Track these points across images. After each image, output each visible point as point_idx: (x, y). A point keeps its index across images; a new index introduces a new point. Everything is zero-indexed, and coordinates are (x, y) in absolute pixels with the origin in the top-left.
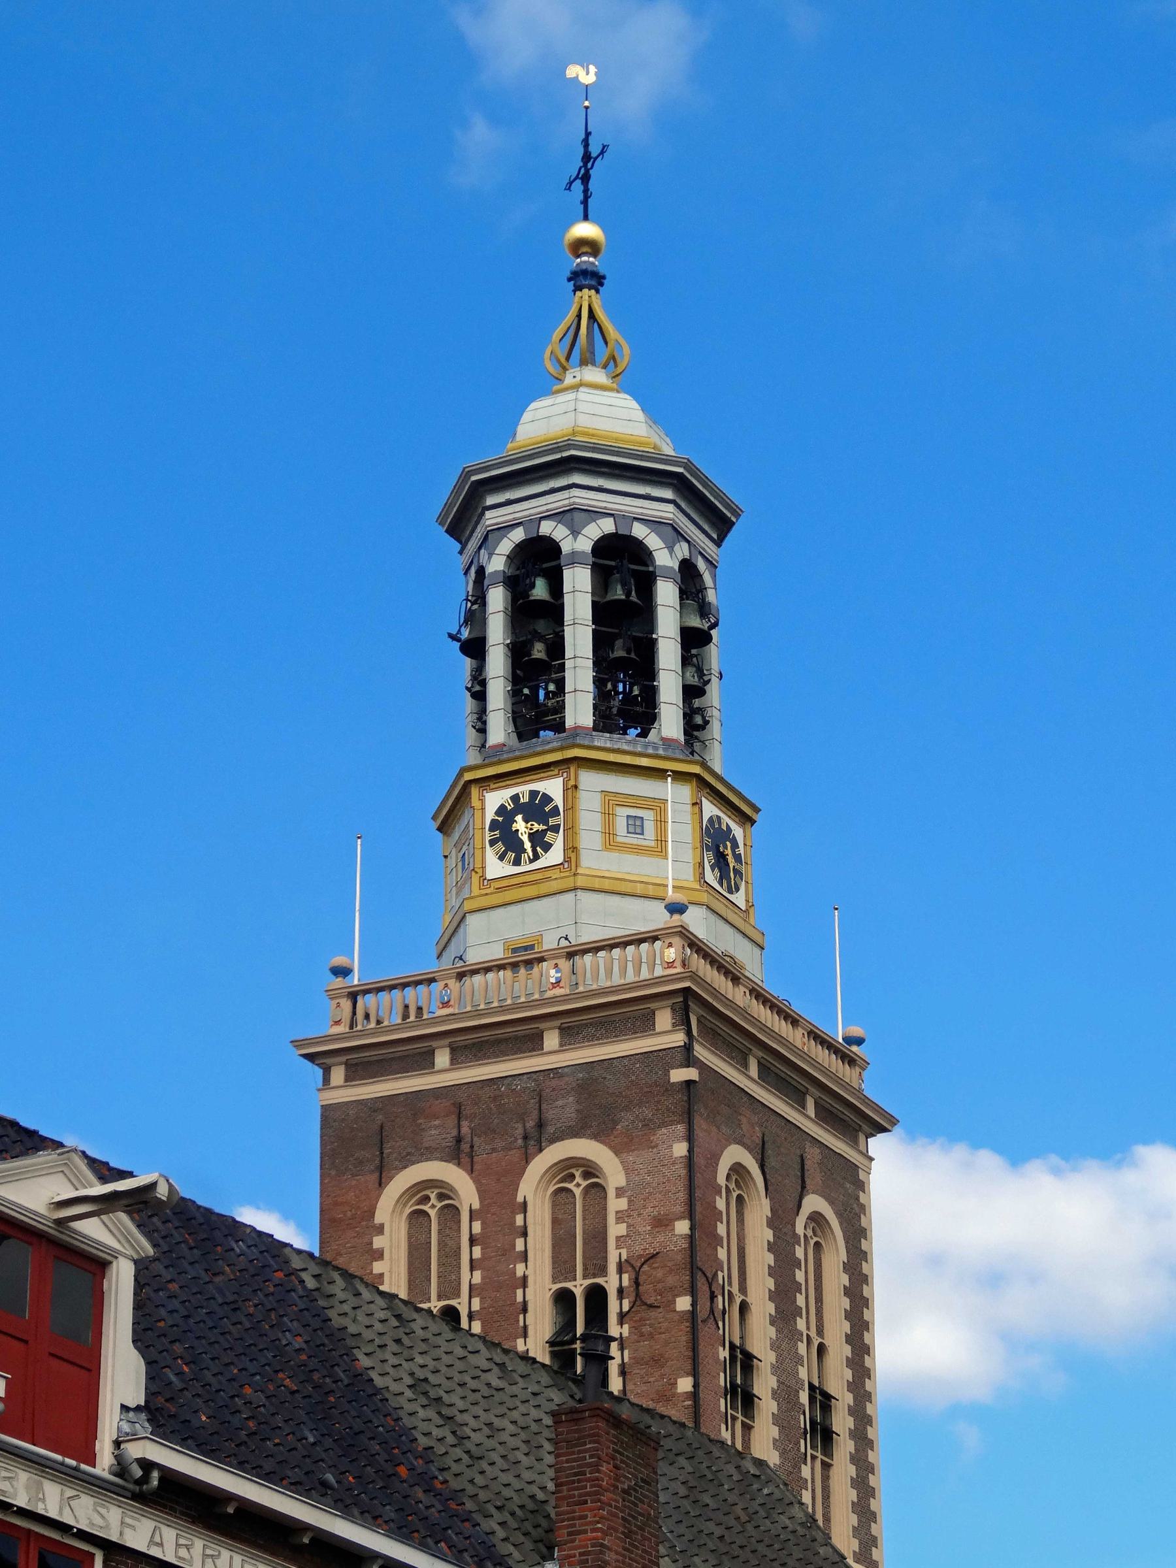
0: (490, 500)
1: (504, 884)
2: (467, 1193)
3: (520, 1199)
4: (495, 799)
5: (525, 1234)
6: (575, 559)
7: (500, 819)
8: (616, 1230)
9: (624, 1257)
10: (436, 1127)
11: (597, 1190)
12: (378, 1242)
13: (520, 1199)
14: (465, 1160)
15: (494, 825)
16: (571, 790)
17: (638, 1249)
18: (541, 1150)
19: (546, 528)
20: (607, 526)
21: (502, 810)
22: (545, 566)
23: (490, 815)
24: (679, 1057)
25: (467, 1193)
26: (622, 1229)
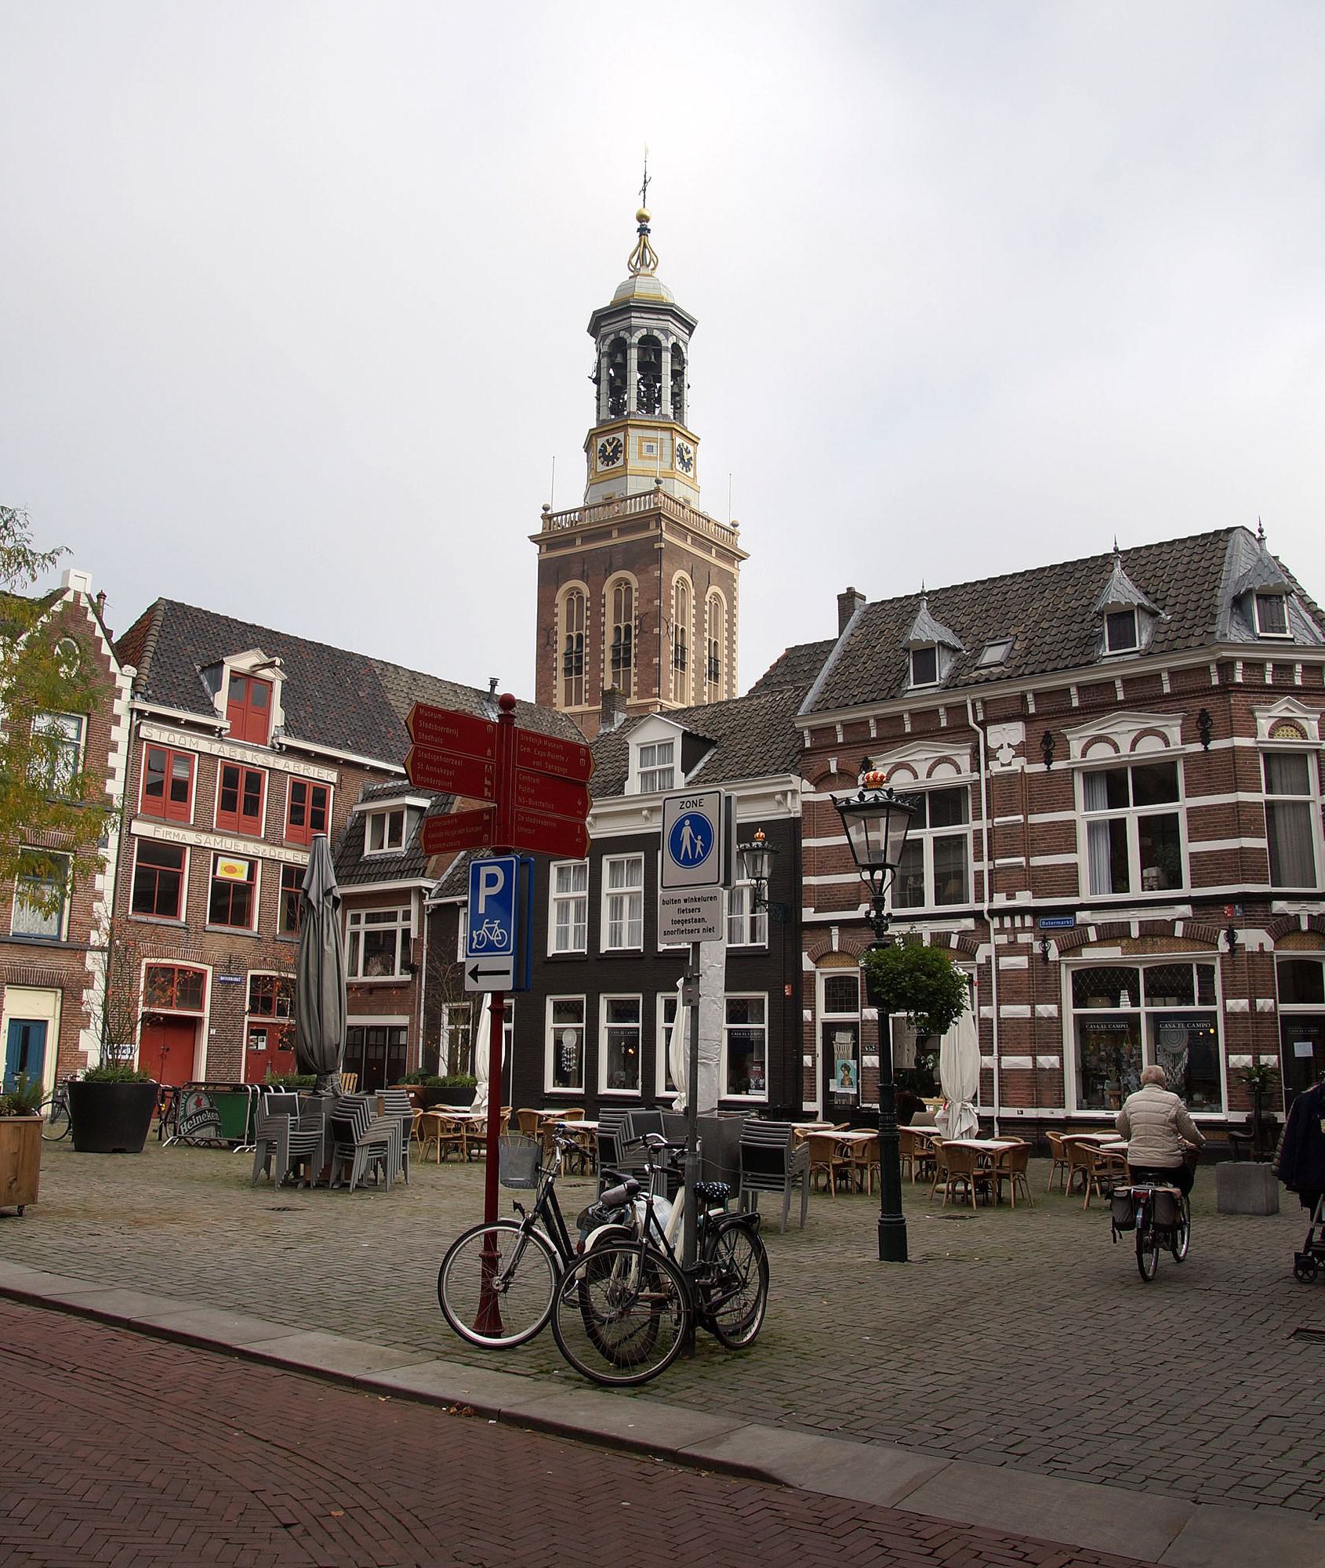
1: (604, 473)
2: (586, 593)
4: (601, 441)
8: (635, 604)
11: (629, 590)
19: (622, 334)
20: (644, 332)
25: (586, 593)
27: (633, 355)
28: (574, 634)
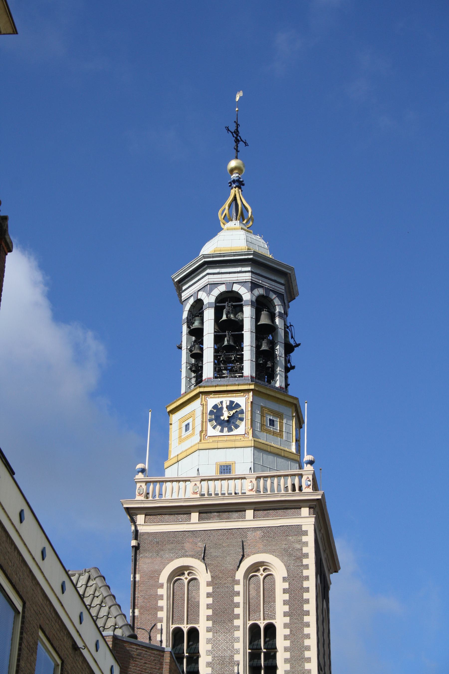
7: (215, 411)
15: (211, 413)
19: (236, 288)
21: (215, 407)
22: (234, 304)
23: (210, 408)
27: (248, 313)
28: (185, 628)
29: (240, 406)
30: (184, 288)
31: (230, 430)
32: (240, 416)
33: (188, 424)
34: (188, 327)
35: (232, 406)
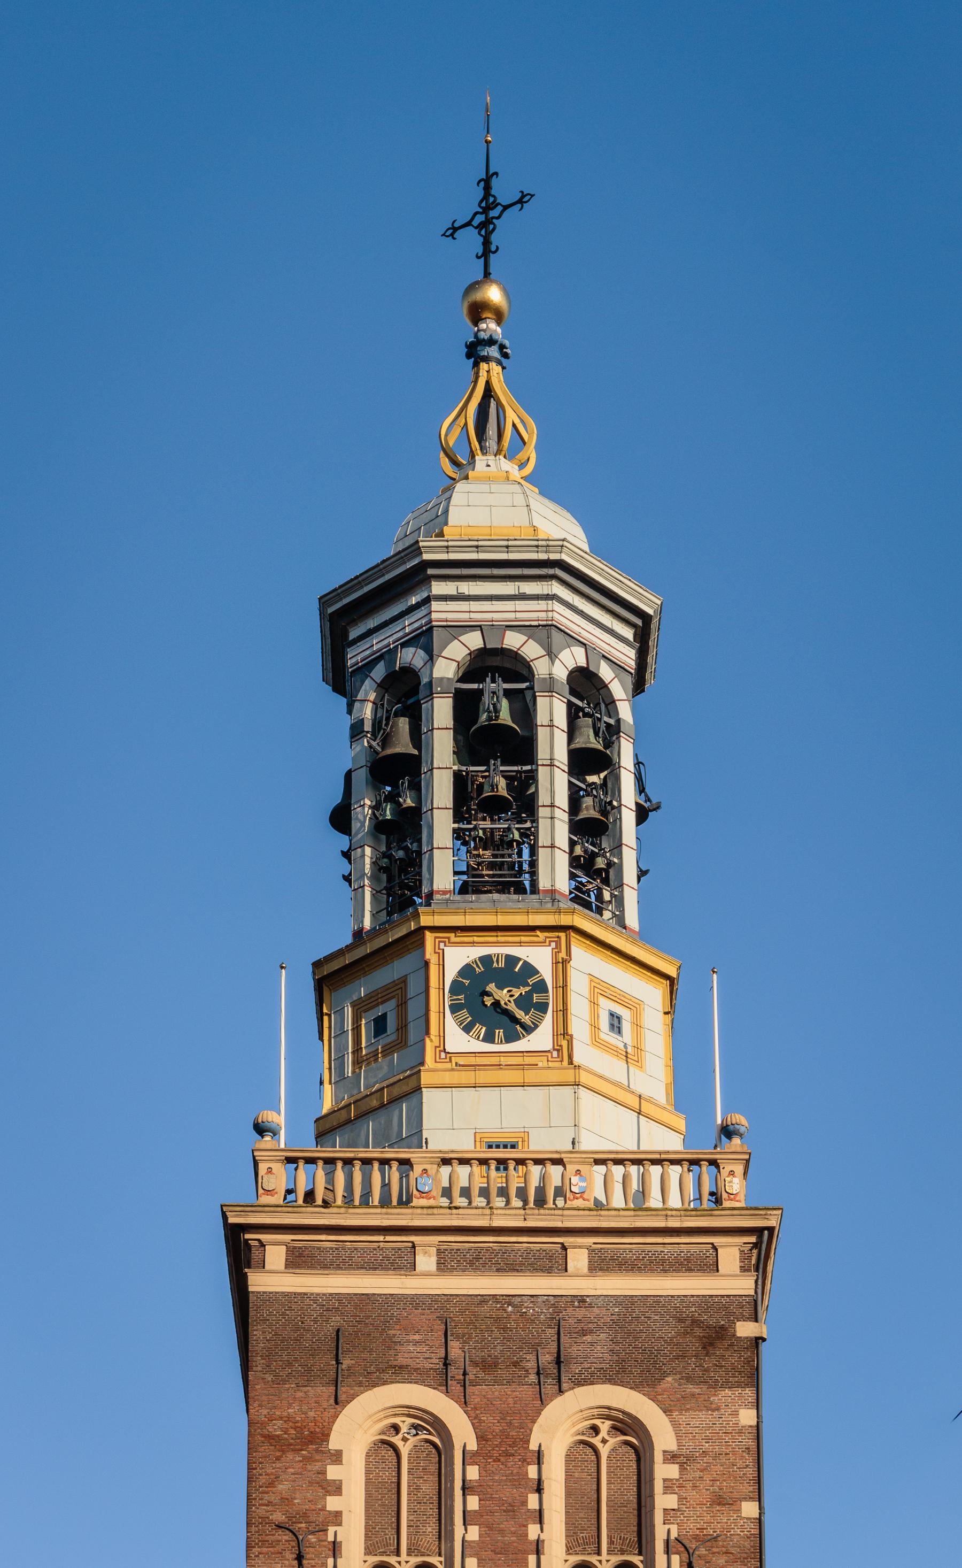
0: (438, 588)
2: (463, 1433)
3: (533, 1446)
5: (539, 1490)
6: (550, 686)
7: (467, 982)
8: (663, 1501)
9: (674, 1534)
10: (416, 1343)
11: (642, 1453)
12: (333, 1472)
13: (533, 1446)
14: (456, 1387)
16: (562, 964)
17: (692, 1527)
18: (561, 1391)
19: (513, 640)
23: (451, 974)
24: (748, 1311)
25: (463, 1433)
26: (671, 1501)
29: (534, 971)
30: (353, 634)
31: (511, 1037)
32: (536, 998)
33: (384, 1016)
34: (570, 740)
35: (516, 973)
